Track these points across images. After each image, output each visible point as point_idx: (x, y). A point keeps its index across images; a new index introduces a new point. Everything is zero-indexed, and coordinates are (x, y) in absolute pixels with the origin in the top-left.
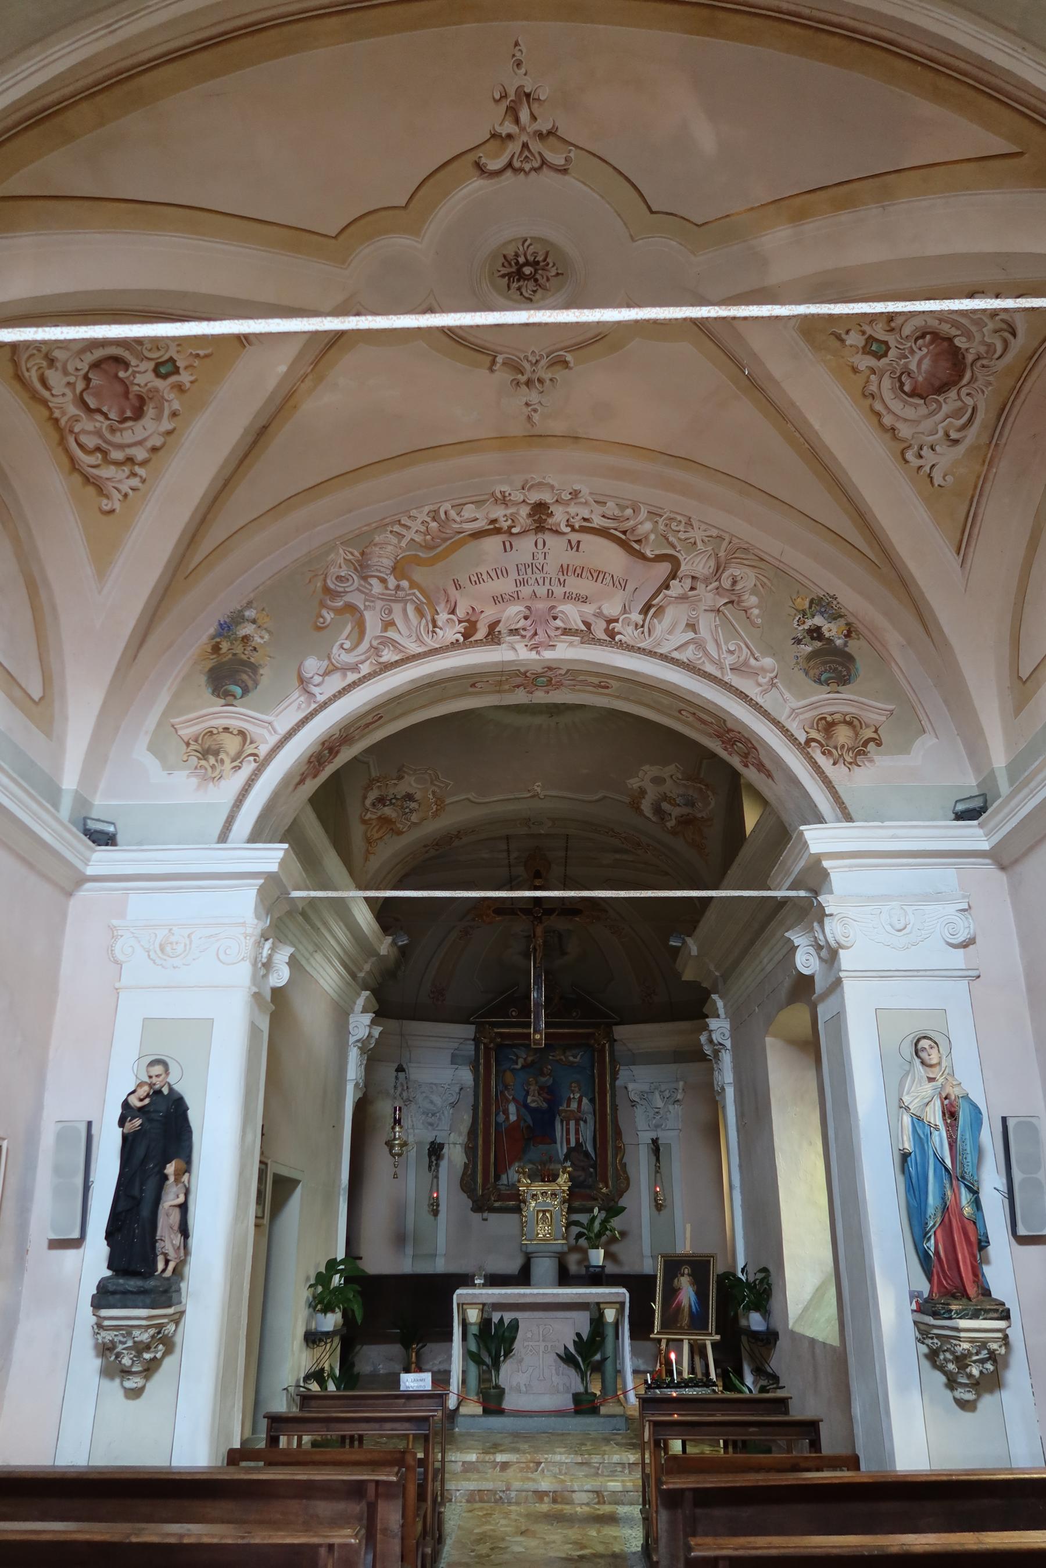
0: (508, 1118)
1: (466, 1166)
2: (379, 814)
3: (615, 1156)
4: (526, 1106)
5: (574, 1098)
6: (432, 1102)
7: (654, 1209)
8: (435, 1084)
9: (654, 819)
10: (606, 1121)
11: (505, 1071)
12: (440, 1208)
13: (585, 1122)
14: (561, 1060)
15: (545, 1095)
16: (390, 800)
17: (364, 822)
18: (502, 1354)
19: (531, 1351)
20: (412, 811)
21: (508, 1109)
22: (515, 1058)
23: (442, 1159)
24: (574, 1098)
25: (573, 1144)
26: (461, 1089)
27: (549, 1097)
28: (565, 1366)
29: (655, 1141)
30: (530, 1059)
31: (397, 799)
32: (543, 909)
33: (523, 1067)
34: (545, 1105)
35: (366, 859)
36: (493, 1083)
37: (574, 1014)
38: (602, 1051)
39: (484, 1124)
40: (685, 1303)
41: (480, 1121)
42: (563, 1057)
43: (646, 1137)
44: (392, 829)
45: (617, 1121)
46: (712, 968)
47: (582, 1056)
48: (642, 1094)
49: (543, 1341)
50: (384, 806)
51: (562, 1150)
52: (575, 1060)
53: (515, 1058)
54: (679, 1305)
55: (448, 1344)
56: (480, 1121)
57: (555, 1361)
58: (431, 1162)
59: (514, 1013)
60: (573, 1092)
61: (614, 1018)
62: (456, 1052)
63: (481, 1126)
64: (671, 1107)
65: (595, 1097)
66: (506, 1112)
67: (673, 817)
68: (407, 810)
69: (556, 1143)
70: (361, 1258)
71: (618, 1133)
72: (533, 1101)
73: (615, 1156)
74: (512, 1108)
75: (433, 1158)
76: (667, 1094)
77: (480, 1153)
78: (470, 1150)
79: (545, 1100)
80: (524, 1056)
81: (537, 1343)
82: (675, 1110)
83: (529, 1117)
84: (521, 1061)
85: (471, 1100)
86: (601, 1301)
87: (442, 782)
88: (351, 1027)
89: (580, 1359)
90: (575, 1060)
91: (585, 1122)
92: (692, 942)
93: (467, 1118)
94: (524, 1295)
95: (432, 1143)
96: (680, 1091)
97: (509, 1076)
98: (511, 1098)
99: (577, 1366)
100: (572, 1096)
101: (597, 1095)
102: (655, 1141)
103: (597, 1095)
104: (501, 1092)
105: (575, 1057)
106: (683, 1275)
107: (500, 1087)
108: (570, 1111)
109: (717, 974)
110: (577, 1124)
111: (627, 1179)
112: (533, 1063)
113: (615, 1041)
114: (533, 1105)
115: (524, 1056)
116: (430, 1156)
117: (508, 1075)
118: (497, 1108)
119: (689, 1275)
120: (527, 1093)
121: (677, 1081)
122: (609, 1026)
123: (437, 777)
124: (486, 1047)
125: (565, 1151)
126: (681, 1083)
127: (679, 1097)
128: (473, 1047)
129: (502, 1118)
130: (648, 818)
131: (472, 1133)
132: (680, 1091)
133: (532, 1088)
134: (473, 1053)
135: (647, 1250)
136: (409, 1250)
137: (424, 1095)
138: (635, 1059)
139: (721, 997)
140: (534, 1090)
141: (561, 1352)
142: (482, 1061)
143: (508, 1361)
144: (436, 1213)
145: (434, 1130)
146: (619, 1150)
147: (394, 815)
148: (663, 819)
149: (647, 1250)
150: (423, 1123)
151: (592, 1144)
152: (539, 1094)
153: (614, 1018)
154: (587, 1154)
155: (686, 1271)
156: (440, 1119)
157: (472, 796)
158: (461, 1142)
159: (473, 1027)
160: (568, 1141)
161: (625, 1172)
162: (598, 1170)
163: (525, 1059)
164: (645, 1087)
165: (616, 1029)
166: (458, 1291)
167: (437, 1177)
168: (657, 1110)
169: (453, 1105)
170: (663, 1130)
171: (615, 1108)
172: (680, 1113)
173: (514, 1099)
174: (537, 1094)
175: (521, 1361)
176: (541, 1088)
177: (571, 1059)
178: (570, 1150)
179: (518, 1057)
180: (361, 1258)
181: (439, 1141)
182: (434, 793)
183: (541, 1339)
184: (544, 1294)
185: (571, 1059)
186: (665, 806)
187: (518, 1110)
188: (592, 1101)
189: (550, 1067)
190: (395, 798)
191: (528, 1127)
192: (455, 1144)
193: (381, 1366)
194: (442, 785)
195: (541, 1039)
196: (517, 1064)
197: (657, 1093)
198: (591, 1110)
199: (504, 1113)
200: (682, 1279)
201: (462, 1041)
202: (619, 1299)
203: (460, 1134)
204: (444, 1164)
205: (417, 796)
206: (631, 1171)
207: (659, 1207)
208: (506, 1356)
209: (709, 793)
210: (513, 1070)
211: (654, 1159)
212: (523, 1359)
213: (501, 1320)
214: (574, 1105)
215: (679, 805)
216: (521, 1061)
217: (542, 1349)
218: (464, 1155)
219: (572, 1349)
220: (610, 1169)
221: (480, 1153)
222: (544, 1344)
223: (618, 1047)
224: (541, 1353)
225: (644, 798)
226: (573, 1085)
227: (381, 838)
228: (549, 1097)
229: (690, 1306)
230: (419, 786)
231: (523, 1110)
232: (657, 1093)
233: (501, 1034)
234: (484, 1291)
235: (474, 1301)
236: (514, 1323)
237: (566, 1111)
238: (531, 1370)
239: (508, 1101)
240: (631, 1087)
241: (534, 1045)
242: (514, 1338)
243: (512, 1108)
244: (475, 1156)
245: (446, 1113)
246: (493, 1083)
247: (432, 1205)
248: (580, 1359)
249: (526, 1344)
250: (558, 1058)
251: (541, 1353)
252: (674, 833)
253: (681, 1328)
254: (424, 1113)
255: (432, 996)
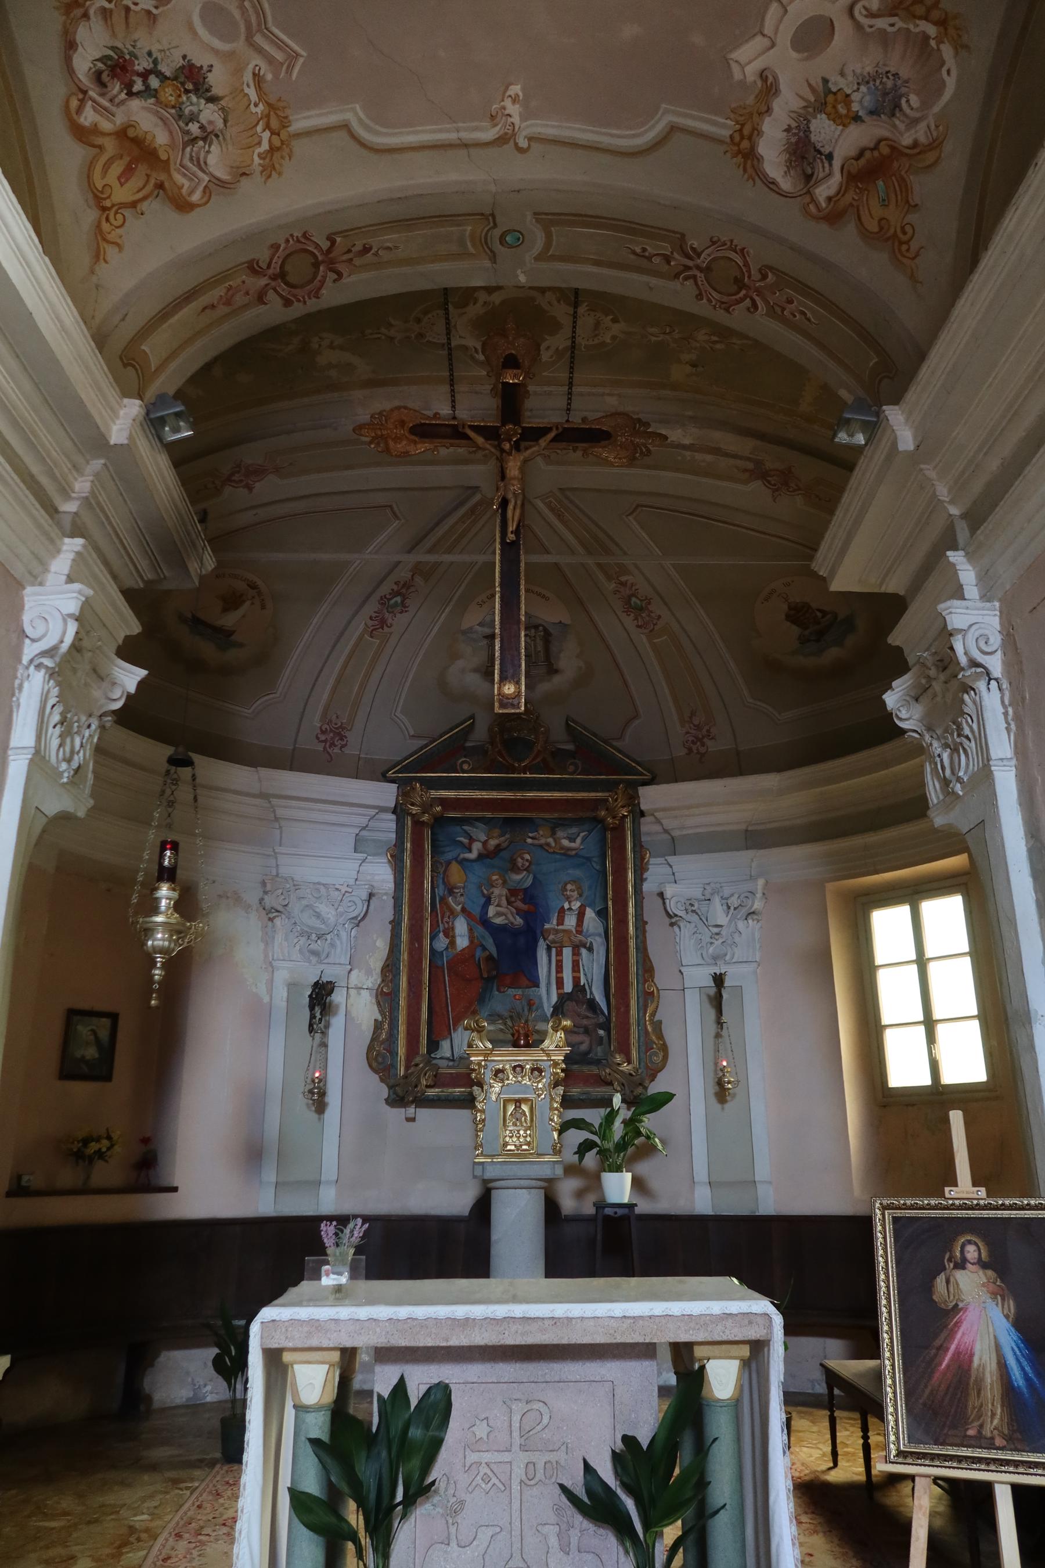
0: (452, 943)
1: (378, 1026)
2: (120, 120)
3: (643, 1008)
4: (485, 922)
5: (570, 909)
6: (318, 915)
7: (713, 1100)
8: (324, 885)
9: (786, 184)
10: (627, 947)
11: (449, 863)
12: (328, 1099)
13: (590, 949)
14: (548, 844)
15: (519, 904)
16: (145, 75)
17: (82, 134)
18: (399, 1496)
19: (486, 1479)
20: (207, 135)
21: (453, 929)
22: (466, 841)
23: (335, 1014)
24: (570, 909)
25: (568, 987)
26: (371, 895)
27: (525, 907)
28: (587, 1524)
29: (719, 980)
30: (493, 843)
31: (163, 77)
32: (524, 428)
33: (481, 857)
34: (519, 921)
35: (98, 256)
36: (427, 885)
37: (571, 768)
38: (619, 830)
39: (410, 954)
40: (984, 1359)
41: (404, 947)
42: (550, 840)
43: (700, 977)
44: (160, 186)
45: (645, 949)
46: (943, 492)
47: (584, 840)
48: (690, 907)
49: (523, 1448)
50: (130, 94)
51: (548, 996)
52: (573, 845)
53: (466, 841)
54: (963, 1363)
55: (236, 1467)
56: (404, 947)
57: (558, 1510)
58: (313, 1017)
59: (466, 767)
60: (568, 899)
61: (642, 774)
62: (364, 833)
63: (405, 956)
64: (741, 925)
65: (607, 908)
66: (449, 933)
67: (837, 164)
68: (194, 128)
69: (538, 986)
70: (175, 1189)
71: (647, 970)
72: (499, 914)
73: (643, 1008)
74: (461, 926)
75: (318, 1011)
76: (734, 901)
77: (402, 1003)
78: (386, 998)
79: (519, 912)
80: (483, 838)
81: (506, 1457)
82: (749, 928)
83: (491, 940)
84: (477, 847)
85: (389, 914)
86: (700, 1337)
87: (280, 45)
88: (26, 618)
89: (630, 1504)
90: (573, 845)
91: (590, 949)
92: (901, 418)
93: (381, 945)
94: (467, 1323)
95: (316, 984)
96: (759, 895)
97: (456, 873)
98: (459, 908)
99: (622, 1528)
100: (566, 906)
101: (610, 903)
102: (719, 980)
103: (610, 903)
104: (443, 899)
105: (572, 840)
106: (961, 1265)
107: (441, 891)
108: (564, 931)
109: (954, 511)
110: (576, 953)
111: (664, 1048)
112: (498, 849)
113: (642, 814)
114: (498, 921)
115: (483, 838)
116: (312, 1008)
117: (455, 867)
118: (435, 926)
119: (983, 1265)
120: (488, 901)
121: (752, 878)
122: (634, 785)
123: (263, 26)
124: (417, 824)
125: (554, 999)
126: (761, 882)
127: (758, 905)
128: (393, 826)
129: (442, 943)
130: (771, 185)
131: (390, 968)
132: (759, 895)
133: (497, 891)
134: (394, 836)
135: (701, 1172)
136: (270, 1175)
137: (304, 902)
138: (674, 846)
139: (970, 556)
140: (500, 896)
141: (576, 1481)
142: (408, 845)
143: (423, 1510)
144: (320, 1106)
145: (321, 963)
146: (649, 997)
147: (161, 138)
148: (808, 178)
149: (701, 1172)
150: (301, 951)
151: (602, 987)
152: (509, 903)
153: (642, 774)
154: (592, 1005)
155: (971, 1252)
156: (333, 945)
157: (354, 114)
158: (370, 985)
159: (394, 787)
160: (560, 983)
161: (661, 1037)
162: (613, 1032)
163: (485, 843)
164: (696, 892)
165: (642, 790)
166: (267, 1313)
167: (324, 1045)
168: (716, 930)
169: (358, 922)
170: (726, 963)
171: (641, 925)
172: (757, 935)
173: (463, 910)
174: (504, 902)
175: (455, 1511)
176: (513, 892)
177: (565, 843)
178: (563, 998)
179: (472, 840)
180: (175, 1189)
181: (325, 979)
182: (258, 78)
183: (517, 1440)
184: (526, 1320)
185: (565, 843)
186: (822, 129)
187: (471, 930)
188: (602, 914)
189: (527, 857)
190: (155, 71)
191: (490, 958)
192: (359, 988)
193: (209, 1388)
194: (279, 56)
195: (518, 695)
196: (470, 851)
197: (717, 901)
198: (601, 930)
199: (446, 935)
200: (960, 1276)
201: (373, 812)
202: (754, 1333)
203: (369, 972)
204: (337, 1023)
205: (218, 80)
206: (671, 1035)
207: (721, 1093)
208: (410, 1501)
209: (947, 51)
210: (463, 862)
211: (712, 1013)
212: (462, 1503)
213: (400, 1388)
214: (570, 922)
215: (857, 118)
216: (477, 847)
217: (519, 1472)
218: (375, 1007)
219: (606, 1472)
220: (634, 1030)
221: (402, 1003)
222: (524, 1457)
223: (647, 826)
224: (516, 1487)
225: (769, 110)
226: (569, 887)
227: (133, 205)
228: (525, 907)
229: (1002, 1366)
230: (217, 43)
231: (480, 930)
232: (717, 901)
233: (443, 802)
234: (344, 1312)
235: (314, 1342)
236: (438, 1395)
237: (557, 931)
238: (485, 1535)
239: (453, 914)
240: (669, 891)
241: (502, 705)
242: (436, 1444)
243: (461, 926)
244: (393, 1009)
245: (344, 935)
246: (427, 885)
247: (311, 1092)
248: (630, 1504)
249: (472, 1457)
250: (542, 841)
251: (516, 1487)
252: (833, 216)
253: (982, 1441)
254: (302, 934)
255: (323, 738)
